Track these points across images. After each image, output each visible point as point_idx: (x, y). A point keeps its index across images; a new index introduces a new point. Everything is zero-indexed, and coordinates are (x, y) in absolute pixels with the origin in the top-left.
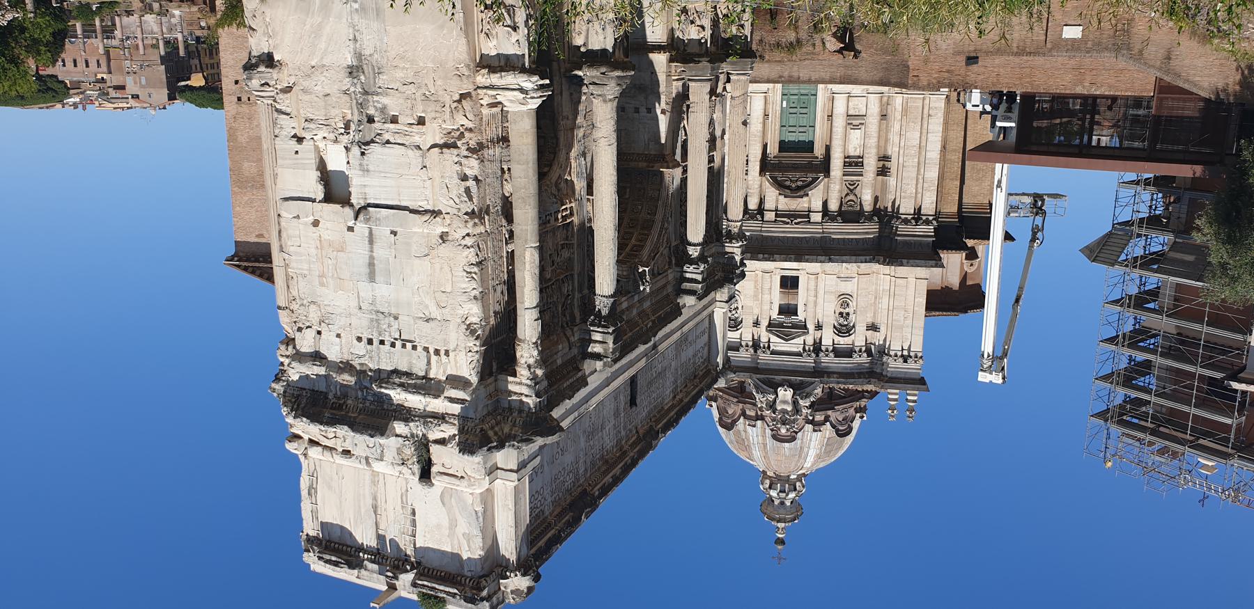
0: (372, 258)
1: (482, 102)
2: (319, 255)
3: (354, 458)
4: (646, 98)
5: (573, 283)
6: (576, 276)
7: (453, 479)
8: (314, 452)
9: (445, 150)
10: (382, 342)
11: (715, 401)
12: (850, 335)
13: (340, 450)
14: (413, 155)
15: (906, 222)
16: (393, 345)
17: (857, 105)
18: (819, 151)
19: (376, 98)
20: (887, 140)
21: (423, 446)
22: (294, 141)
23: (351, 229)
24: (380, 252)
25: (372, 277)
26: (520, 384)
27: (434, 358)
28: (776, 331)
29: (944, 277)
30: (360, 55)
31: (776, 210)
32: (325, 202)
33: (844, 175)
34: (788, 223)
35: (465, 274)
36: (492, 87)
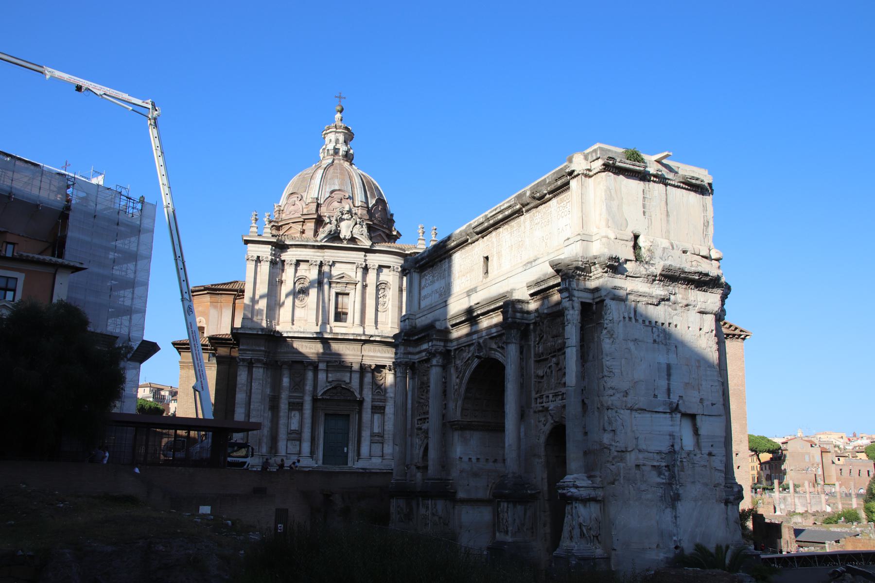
0: (669, 379)
1: (600, 479)
6: (532, 356)
7: (621, 238)
9: (624, 450)
11: (388, 219)
12: (298, 277)
14: (643, 446)
15: (258, 361)
19: (664, 481)
20: (272, 421)
22: (714, 452)
24: (663, 383)
25: (669, 367)
26: (578, 298)
28: (352, 281)
30: (673, 508)
32: (696, 415)
33: (303, 397)
35: (614, 371)
36: (595, 488)
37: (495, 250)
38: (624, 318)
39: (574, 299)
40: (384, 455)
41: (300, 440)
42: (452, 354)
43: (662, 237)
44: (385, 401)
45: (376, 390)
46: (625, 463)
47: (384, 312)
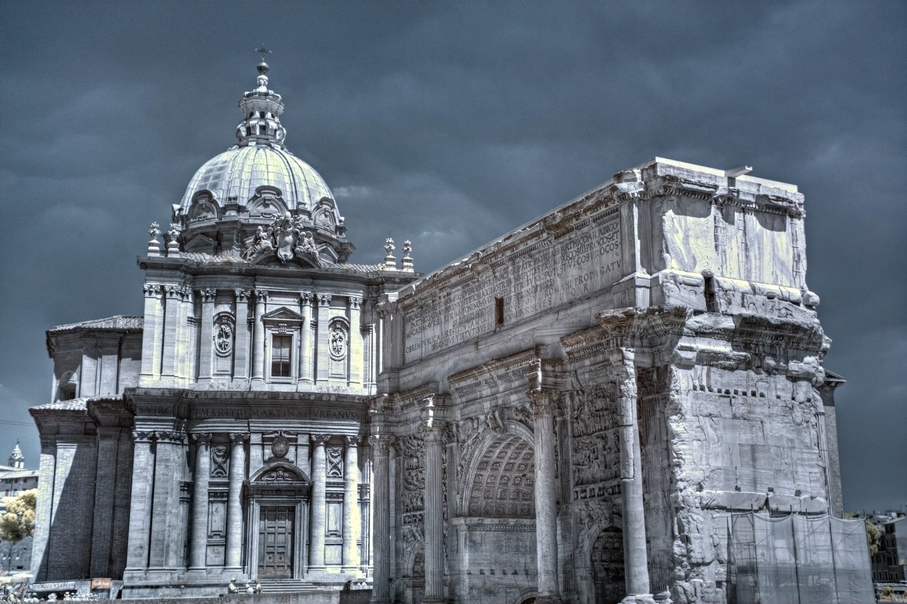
0: (754, 466)
2: (794, 466)
3: (765, 293)
4: (485, 583)
5: (573, 430)
8: (796, 294)
9: (700, 561)
10: (745, 394)
12: (218, 314)
13: (776, 299)
15: (164, 435)
16: (736, 392)
17: (216, 557)
18: (256, 509)
21: (712, 307)
23: (771, 490)
27: (704, 383)
29: (99, 367)
31: (296, 446)
34: (285, 432)
35: (684, 457)
37: (513, 289)
38: (695, 388)
39: (627, 362)
40: (345, 562)
41: (226, 545)
42: (454, 429)
43: (740, 279)
44: (344, 485)
45: (332, 469)
46: (703, 578)
47: (340, 361)
